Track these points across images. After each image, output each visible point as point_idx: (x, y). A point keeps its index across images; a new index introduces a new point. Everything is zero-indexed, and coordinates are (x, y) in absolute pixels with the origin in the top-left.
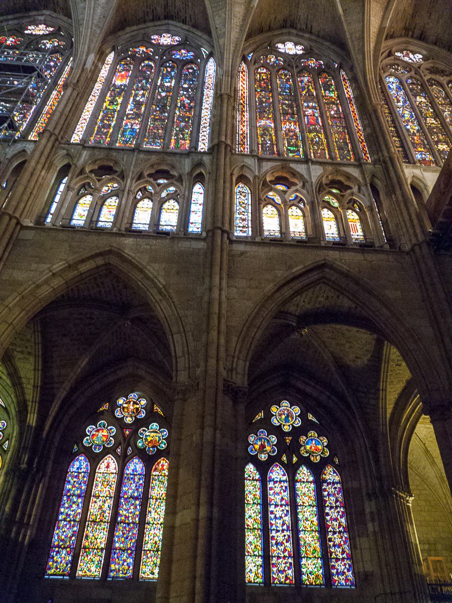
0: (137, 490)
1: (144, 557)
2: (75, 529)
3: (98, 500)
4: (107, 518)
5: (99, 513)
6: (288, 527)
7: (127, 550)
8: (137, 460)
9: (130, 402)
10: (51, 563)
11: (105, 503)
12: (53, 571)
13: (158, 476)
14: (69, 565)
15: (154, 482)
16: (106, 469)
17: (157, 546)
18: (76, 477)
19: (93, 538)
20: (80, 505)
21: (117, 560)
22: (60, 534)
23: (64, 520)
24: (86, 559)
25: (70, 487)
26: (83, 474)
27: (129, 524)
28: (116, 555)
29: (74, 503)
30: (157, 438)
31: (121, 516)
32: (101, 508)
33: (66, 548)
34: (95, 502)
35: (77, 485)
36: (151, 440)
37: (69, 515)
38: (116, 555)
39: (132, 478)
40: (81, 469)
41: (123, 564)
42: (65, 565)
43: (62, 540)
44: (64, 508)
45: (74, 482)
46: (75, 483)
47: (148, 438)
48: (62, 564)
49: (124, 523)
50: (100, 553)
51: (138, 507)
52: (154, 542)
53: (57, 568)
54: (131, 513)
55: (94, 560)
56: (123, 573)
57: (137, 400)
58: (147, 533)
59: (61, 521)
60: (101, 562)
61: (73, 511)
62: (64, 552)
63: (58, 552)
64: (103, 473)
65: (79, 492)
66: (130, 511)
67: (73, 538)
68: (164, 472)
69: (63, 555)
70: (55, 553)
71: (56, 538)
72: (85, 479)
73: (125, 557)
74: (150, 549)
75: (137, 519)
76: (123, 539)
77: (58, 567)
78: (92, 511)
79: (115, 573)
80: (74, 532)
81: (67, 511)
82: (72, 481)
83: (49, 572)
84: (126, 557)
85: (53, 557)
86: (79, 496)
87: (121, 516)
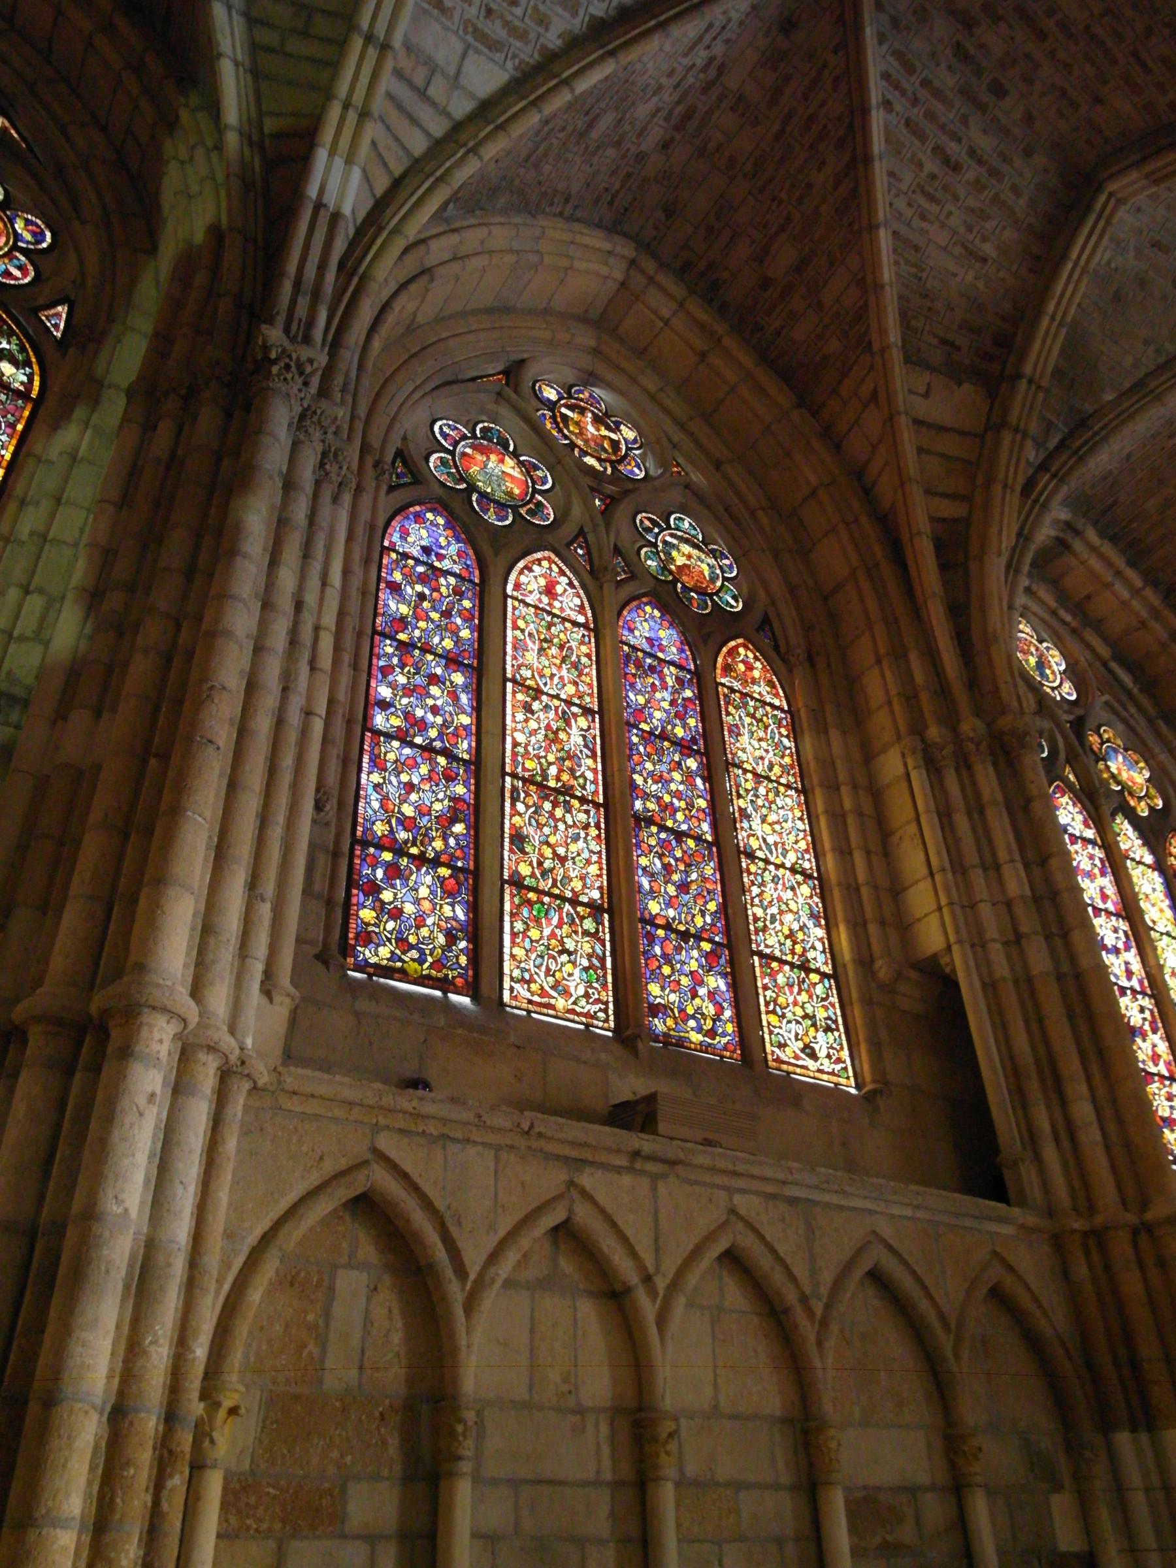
0: (681, 716)
1: (766, 980)
2: (460, 790)
3: (536, 706)
4: (590, 788)
5: (551, 758)
6: (1141, 982)
7: (698, 938)
8: (657, 613)
9: (582, 411)
10: (367, 914)
11: (568, 723)
12: (384, 952)
13: (744, 695)
14: (463, 944)
15: (731, 709)
16: (545, 600)
17: (798, 949)
18: (423, 579)
19: (548, 852)
20: (464, 698)
21: (666, 970)
22: (392, 791)
23: (403, 737)
24: (534, 934)
25: (404, 609)
26: (452, 580)
27: (680, 836)
28: (658, 950)
29: (434, 679)
30: (705, 567)
31: (646, 796)
32: (556, 740)
33: (436, 863)
34: (528, 708)
35: (435, 616)
36: (685, 565)
37: (422, 725)
38: (658, 950)
39: (652, 669)
40: (440, 557)
41: (695, 995)
42: (441, 939)
43: (406, 823)
44: (393, 686)
45: (421, 597)
46: (426, 605)
47: (674, 553)
48: (424, 932)
49: (663, 828)
50: (589, 924)
51: (699, 781)
52: (787, 932)
53: (402, 943)
54: (678, 795)
55: (570, 945)
56: (699, 1030)
57: (606, 414)
58: (755, 890)
59: (389, 736)
60: (602, 960)
61: (435, 710)
62: (428, 880)
63: (393, 872)
64: (536, 607)
65: (448, 644)
66: (673, 787)
67: (459, 828)
68: (756, 688)
69: (424, 892)
70: (380, 873)
71: (376, 805)
72: (467, 604)
73: (694, 965)
74: (777, 953)
75: (705, 827)
76: (671, 890)
77: (412, 939)
78: (520, 738)
79: (670, 1022)
80: (455, 799)
81: (405, 701)
82: (409, 590)
83: (367, 953)
84: (701, 966)
85: (373, 889)
86: (452, 661)
87: (646, 796)
